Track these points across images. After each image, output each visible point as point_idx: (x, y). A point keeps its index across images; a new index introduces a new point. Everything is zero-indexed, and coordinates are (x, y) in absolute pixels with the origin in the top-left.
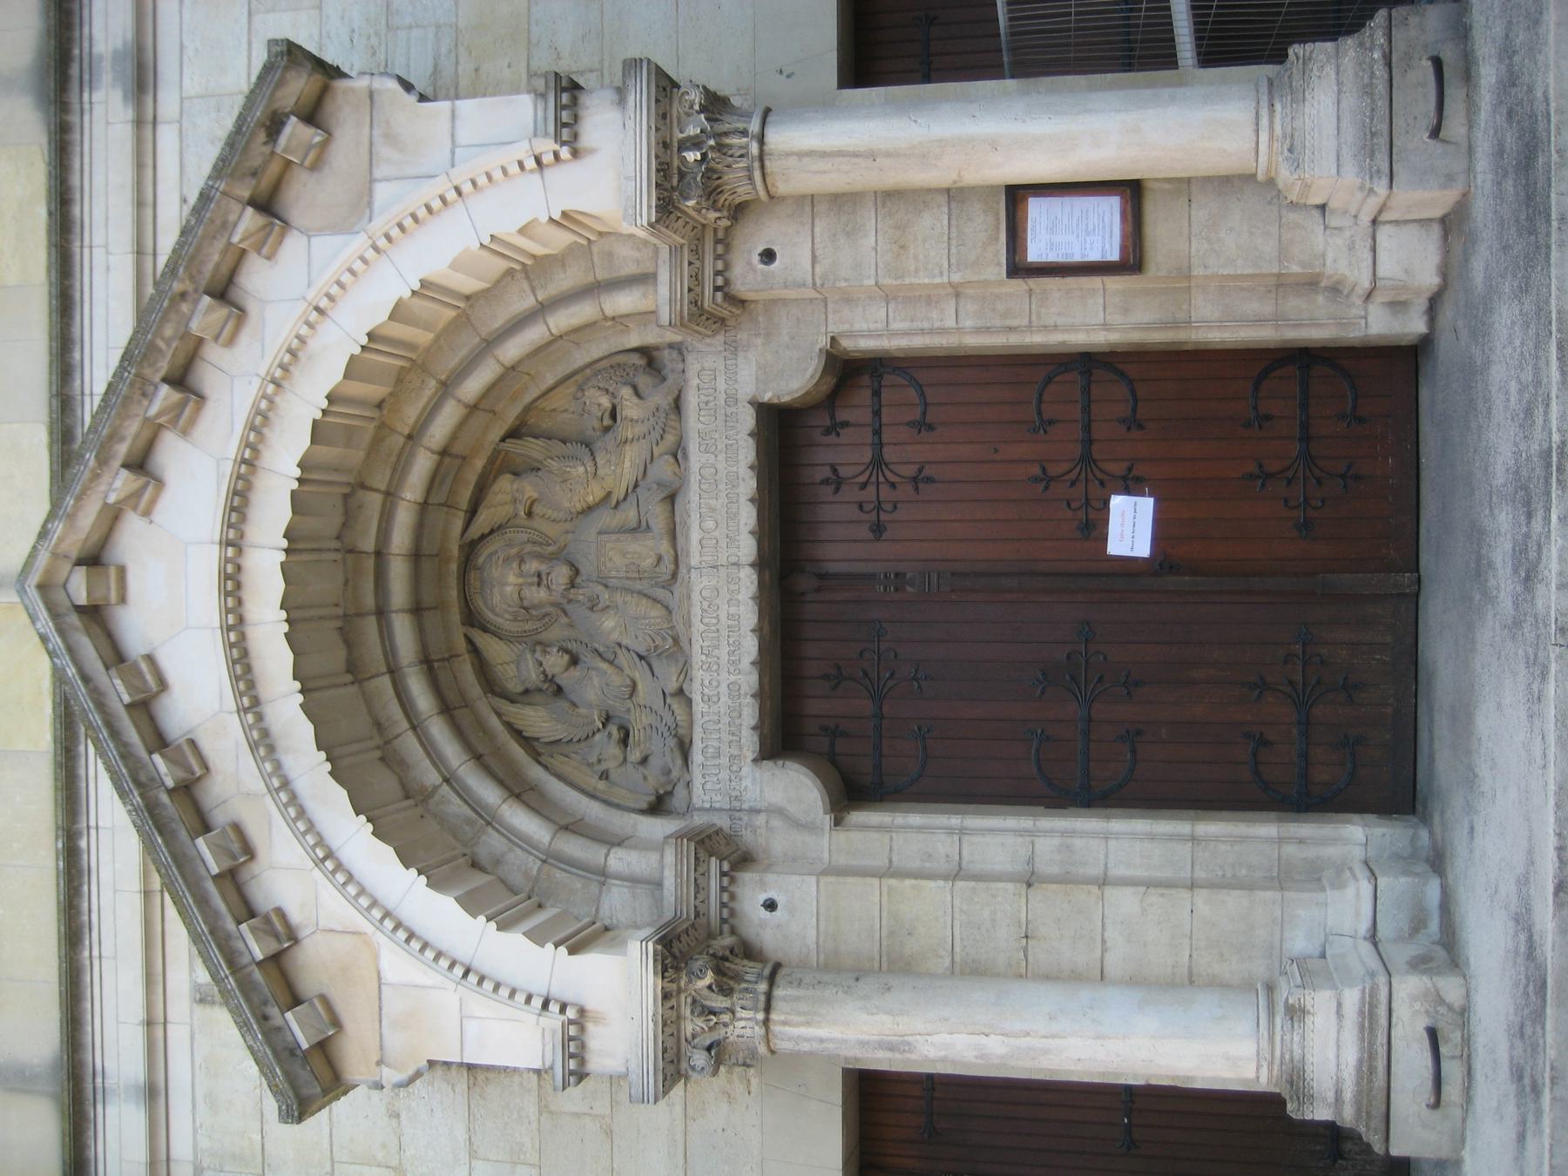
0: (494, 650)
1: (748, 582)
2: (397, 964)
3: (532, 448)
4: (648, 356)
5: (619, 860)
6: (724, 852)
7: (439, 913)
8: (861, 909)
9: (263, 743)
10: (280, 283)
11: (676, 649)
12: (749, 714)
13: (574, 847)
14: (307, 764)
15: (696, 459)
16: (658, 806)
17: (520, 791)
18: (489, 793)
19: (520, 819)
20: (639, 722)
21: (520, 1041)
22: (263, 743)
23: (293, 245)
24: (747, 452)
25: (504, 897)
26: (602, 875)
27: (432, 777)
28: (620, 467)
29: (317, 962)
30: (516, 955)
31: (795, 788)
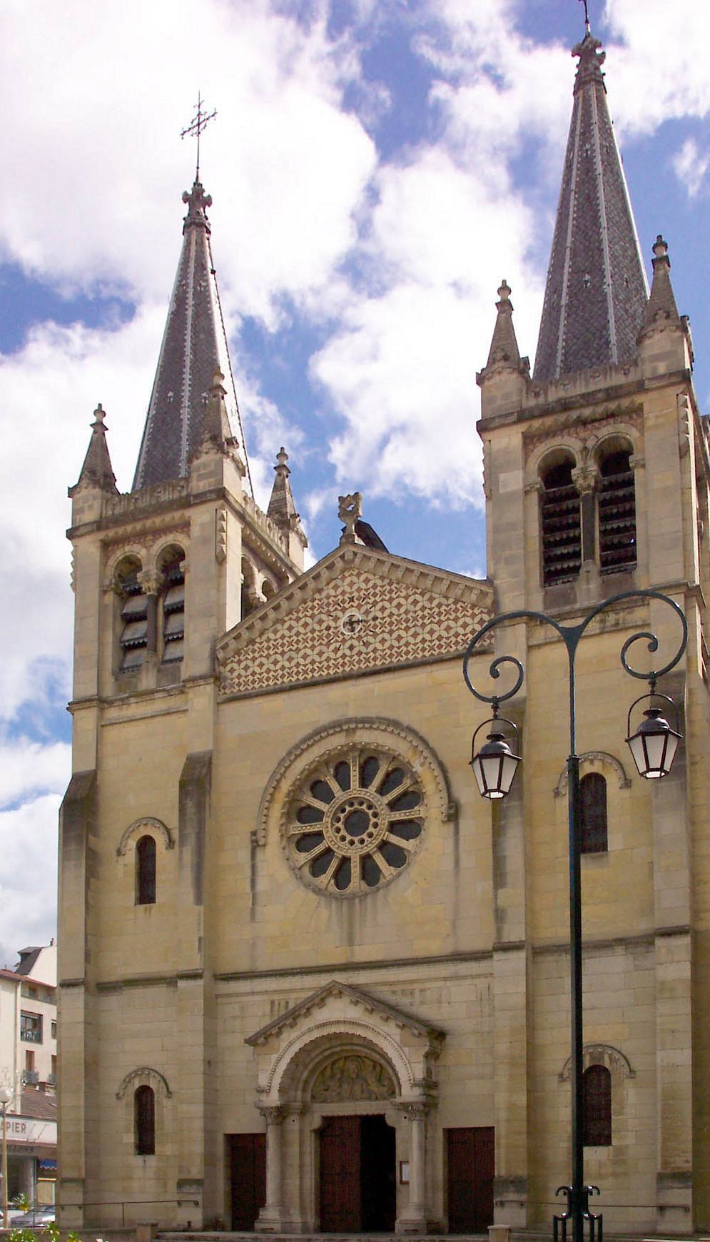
0: (341, 1063)
1: (353, 1113)
2: (274, 1057)
3: (378, 1069)
4: (394, 1092)
5: (299, 1093)
6: (304, 1111)
7: (283, 1066)
8: (294, 1137)
9: (310, 1030)
10: (392, 1029)
11: (341, 1100)
12: (330, 1114)
13: (301, 1085)
14: (307, 1039)
15: (374, 1103)
16: (313, 1097)
17: (312, 1072)
18: (310, 1067)
19: (305, 1074)
20: (328, 1093)
21: (263, 1081)
22: (310, 1030)
23: (398, 1031)
24: (376, 1113)
25: (291, 1074)
26: (296, 1090)
27: (313, 1055)
28: (374, 1087)
29: (273, 1041)
30: (277, 1080)
31: (317, 1122)
